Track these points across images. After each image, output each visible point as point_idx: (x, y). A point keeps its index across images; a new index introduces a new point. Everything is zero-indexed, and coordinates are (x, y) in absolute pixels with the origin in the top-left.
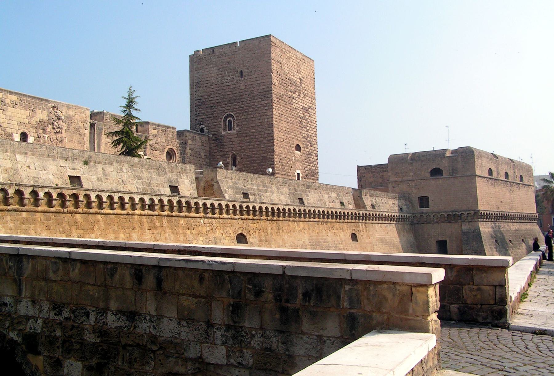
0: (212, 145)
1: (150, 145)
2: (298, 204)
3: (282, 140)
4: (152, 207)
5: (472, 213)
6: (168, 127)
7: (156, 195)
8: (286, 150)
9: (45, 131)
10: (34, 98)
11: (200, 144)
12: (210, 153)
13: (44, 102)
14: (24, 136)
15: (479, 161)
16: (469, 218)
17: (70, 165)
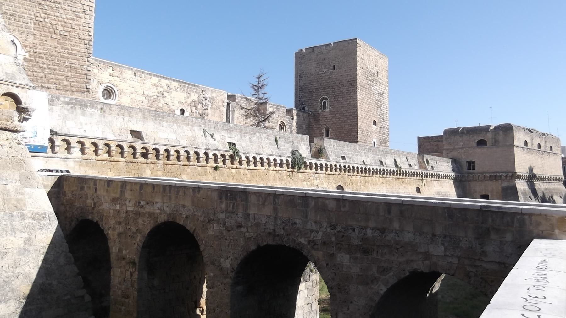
0: (311, 120)
2: (379, 165)
4: (281, 165)
5: (510, 174)
6: (280, 107)
7: (284, 157)
10: (189, 84)
11: (303, 119)
12: (309, 125)
13: (196, 88)
14: (182, 111)
15: (518, 135)
16: (508, 178)
17: (229, 135)
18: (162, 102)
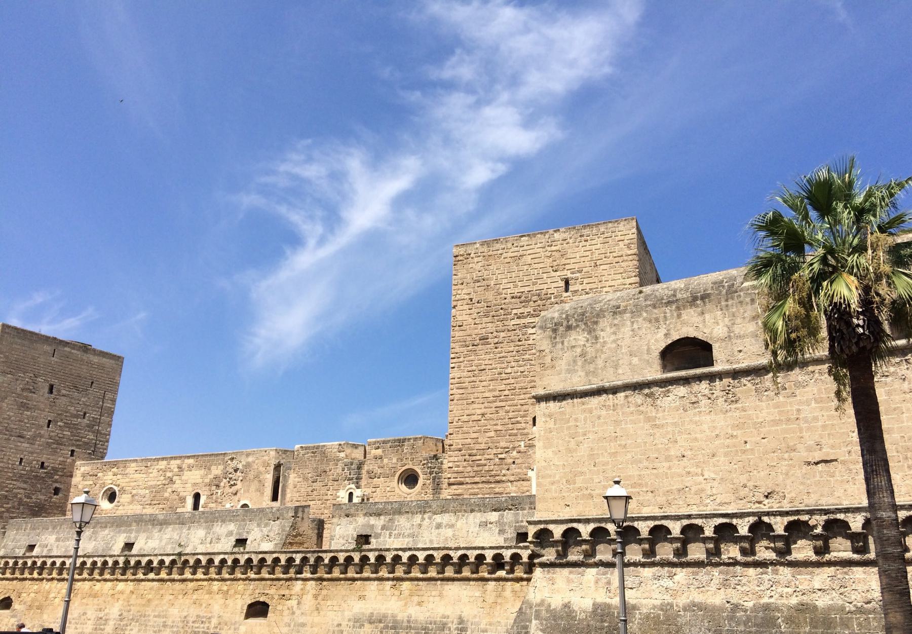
1: (368, 472)
3: (475, 417)
6: (404, 440)
8: (492, 434)
9: (218, 486)
13: (222, 457)
14: (197, 497)
18: (169, 490)
